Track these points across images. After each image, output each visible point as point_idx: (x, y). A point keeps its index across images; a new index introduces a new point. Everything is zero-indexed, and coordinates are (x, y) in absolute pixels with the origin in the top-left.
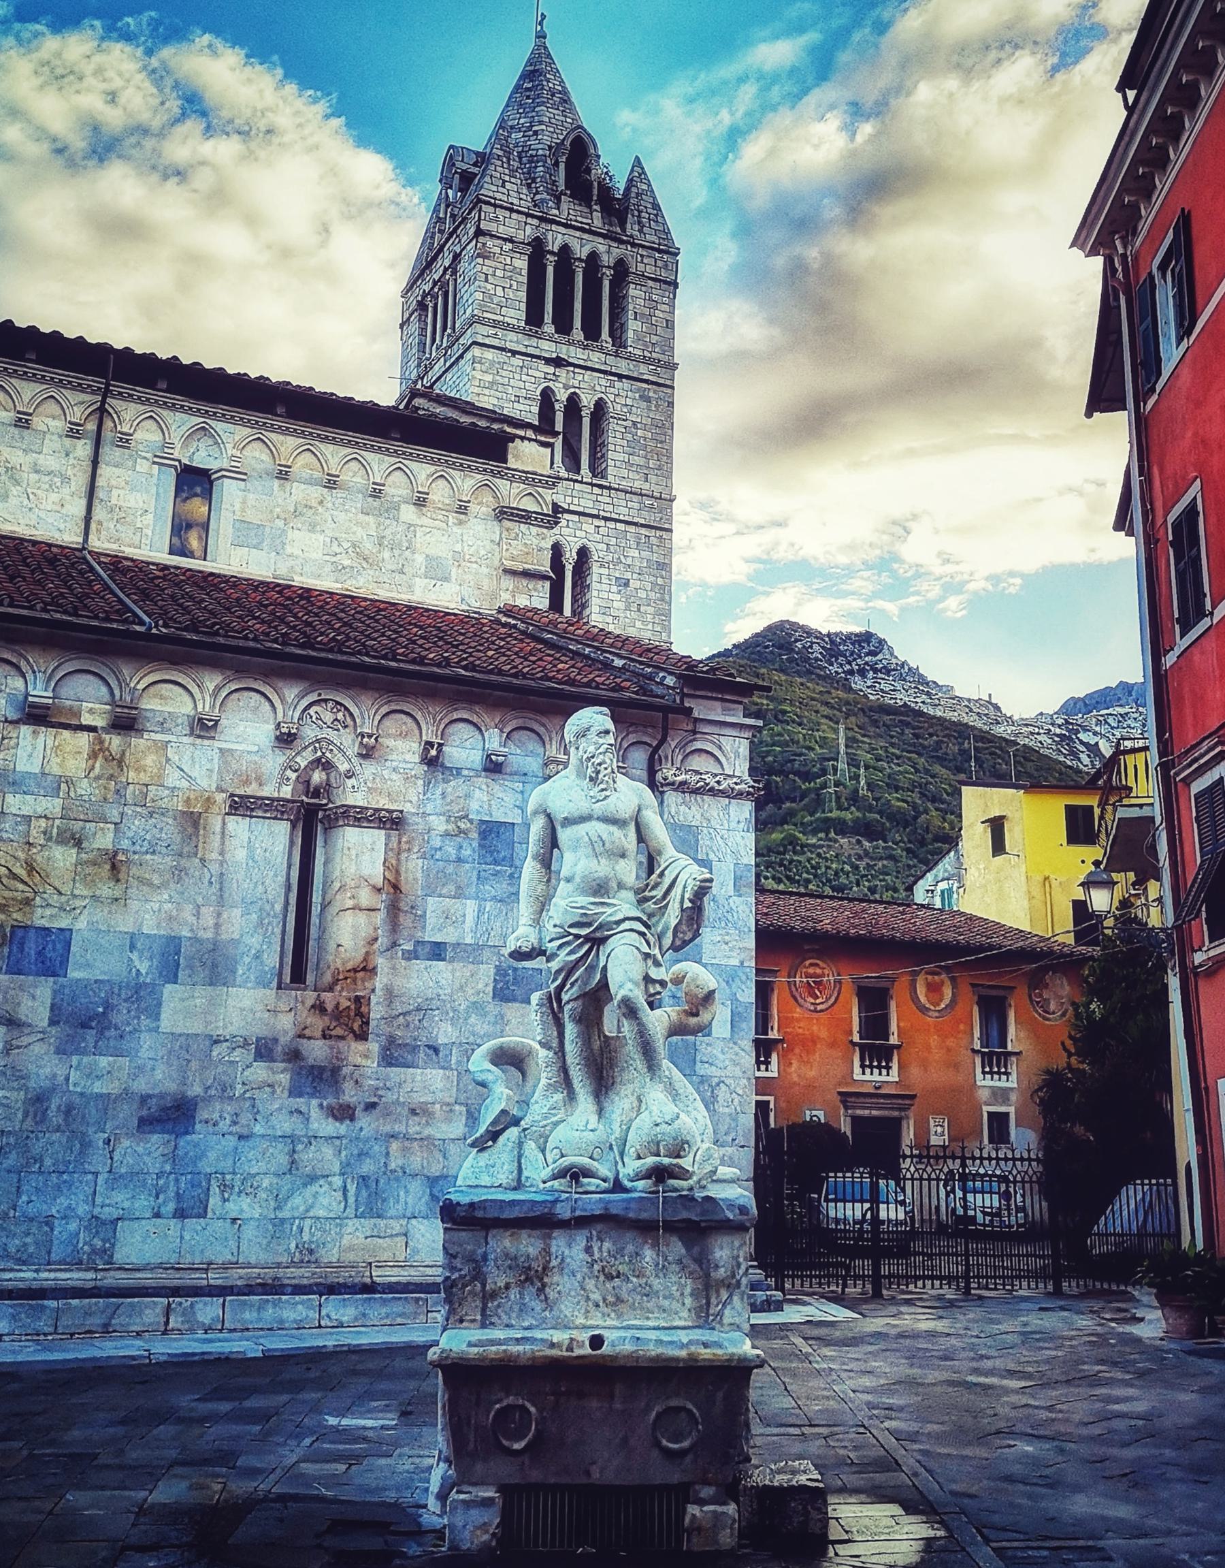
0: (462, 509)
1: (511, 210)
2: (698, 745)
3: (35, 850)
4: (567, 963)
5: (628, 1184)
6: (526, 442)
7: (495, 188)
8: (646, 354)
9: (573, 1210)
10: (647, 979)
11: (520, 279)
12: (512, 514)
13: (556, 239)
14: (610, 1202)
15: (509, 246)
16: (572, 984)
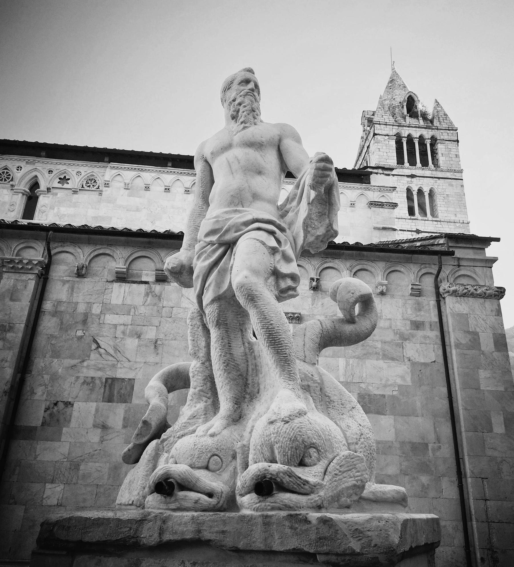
1: (386, 125)
2: (462, 272)
6: (379, 175)
7: (379, 118)
8: (449, 168)
10: (276, 274)
11: (393, 148)
15: (387, 137)
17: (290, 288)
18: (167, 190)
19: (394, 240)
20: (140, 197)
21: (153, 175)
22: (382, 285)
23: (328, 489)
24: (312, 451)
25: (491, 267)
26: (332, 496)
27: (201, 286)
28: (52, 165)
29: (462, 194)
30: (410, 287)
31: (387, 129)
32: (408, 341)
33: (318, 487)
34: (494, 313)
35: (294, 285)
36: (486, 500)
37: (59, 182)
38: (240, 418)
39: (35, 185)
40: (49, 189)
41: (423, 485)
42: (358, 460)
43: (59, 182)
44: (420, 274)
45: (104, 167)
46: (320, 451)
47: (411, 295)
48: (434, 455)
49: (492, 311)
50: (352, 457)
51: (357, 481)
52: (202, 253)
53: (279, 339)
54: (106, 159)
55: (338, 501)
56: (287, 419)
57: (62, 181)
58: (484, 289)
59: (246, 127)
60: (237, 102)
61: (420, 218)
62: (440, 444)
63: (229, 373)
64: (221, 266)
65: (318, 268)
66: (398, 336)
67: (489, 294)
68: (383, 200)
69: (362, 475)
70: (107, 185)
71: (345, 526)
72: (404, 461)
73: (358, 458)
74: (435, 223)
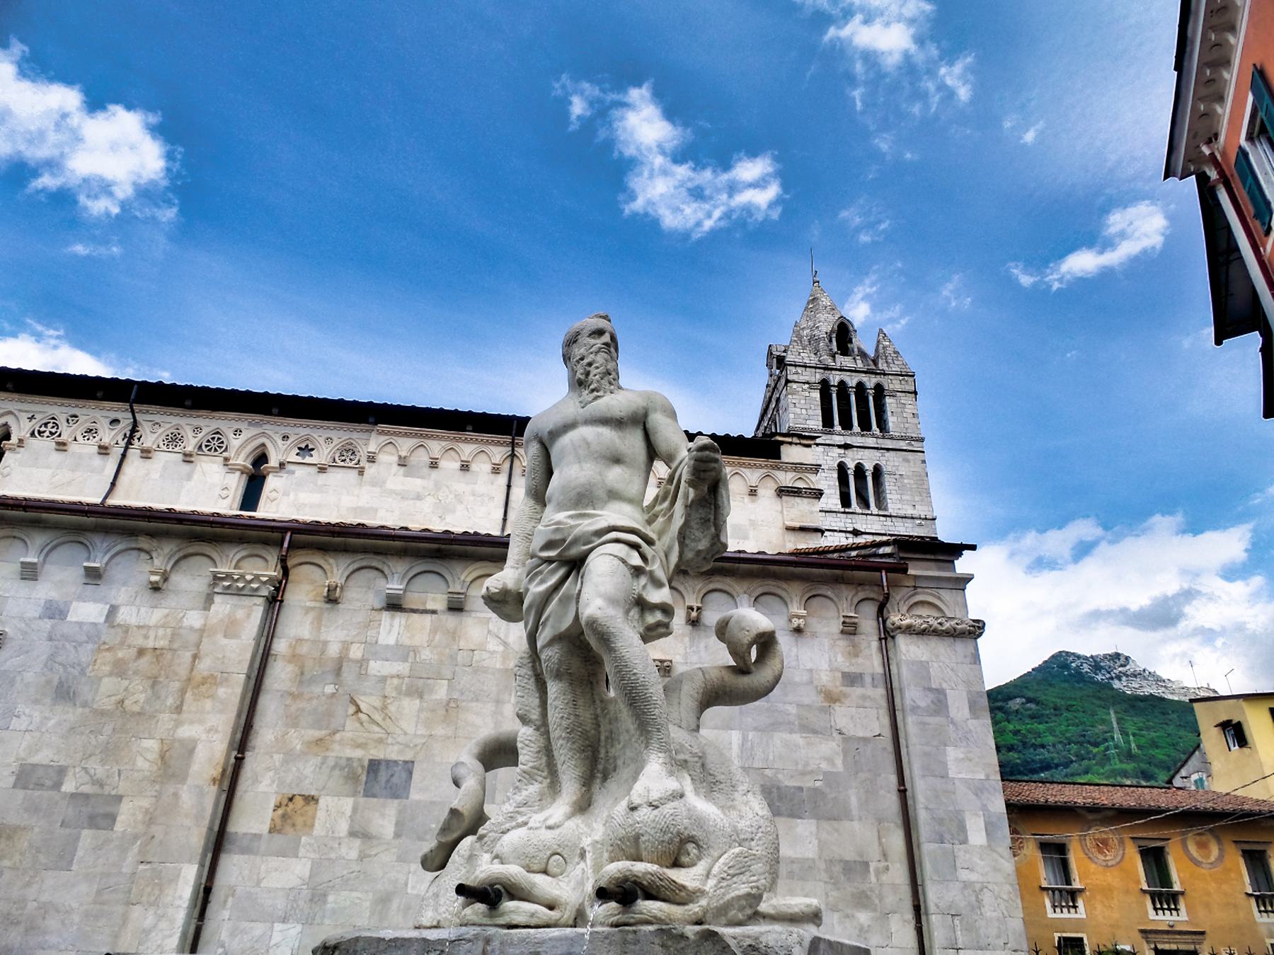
0: (753, 492)
1: (806, 367)
3: (389, 701)
4: (535, 595)
6: (794, 446)
10: (642, 605)
12: (788, 491)
13: (835, 379)
14: (542, 943)
15: (807, 386)
17: (659, 625)
18: (465, 467)
19: (819, 546)
20: (423, 478)
21: (444, 443)
22: (799, 617)
23: (711, 898)
24: (690, 847)
25: (964, 590)
26: (716, 907)
27: (535, 619)
28: (289, 428)
29: (924, 474)
30: (842, 619)
31: (807, 373)
33: (698, 894)
34: (968, 660)
35: (666, 620)
36: (957, 949)
37: (297, 454)
38: (590, 805)
39: (261, 459)
40: (282, 465)
41: (861, 929)
42: (754, 859)
43: (297, 454)
44: (856, 601)
45: (367, 431)
46: (702, 847)
48: (878, 880)
49: (965, 657)
50: (746, 855)
51: (752, 888)
52: (536, 574)
53: (646, 694)
54: (371, 420)
55: (726, 914)
56: (654, 803)
57: (301, 452)
58: (953, 623)
59: (599, 397)
60: (586, 361)
61: (859, 510)
62: (886, 864)
63: (574, 743)
64: (563, 593)
65: (700, 590)
67: (961, 629)
68: (800, 485)
69: (758, 880)
70: (372, 460)
71: (735, 941)
72: (831, 890)
73: (753, 857)
74: (882, 518)
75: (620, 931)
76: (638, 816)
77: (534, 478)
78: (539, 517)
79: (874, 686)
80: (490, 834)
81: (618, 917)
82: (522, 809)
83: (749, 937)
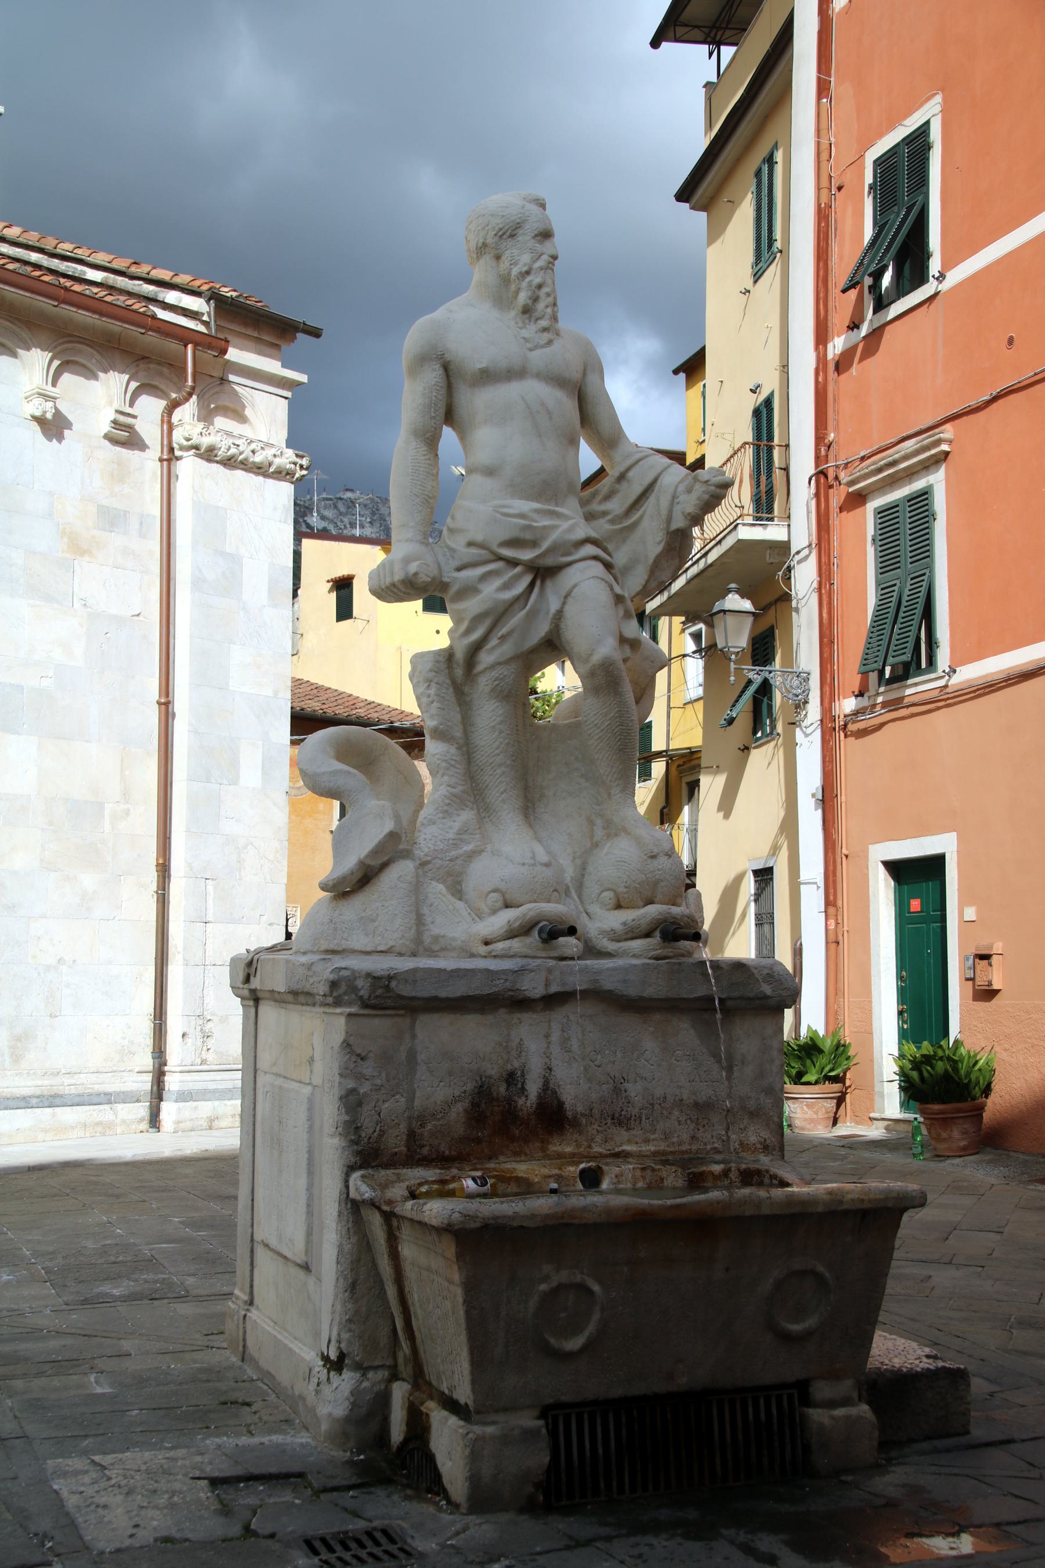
5: (611, 946)
9: (547, 984)
14: (599, 972)
16: (503, 638)
30: (112, 416)
32: (87, 558)
47: (107, 437)
49: (275, 509)
64: (532, 607)
66: (65, 540)
75: (667, 963)
76: (655, 864)
77: (434, 418)
78: (434, 472)
79: (142, 535)
80: (435, 861)
81: (659, 951)
82: (465, 837)
83: (765, 968)
